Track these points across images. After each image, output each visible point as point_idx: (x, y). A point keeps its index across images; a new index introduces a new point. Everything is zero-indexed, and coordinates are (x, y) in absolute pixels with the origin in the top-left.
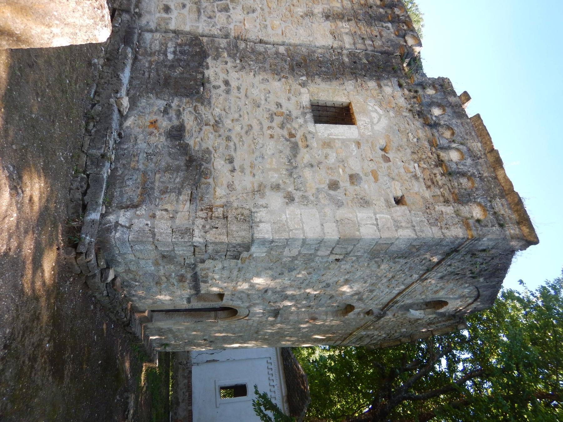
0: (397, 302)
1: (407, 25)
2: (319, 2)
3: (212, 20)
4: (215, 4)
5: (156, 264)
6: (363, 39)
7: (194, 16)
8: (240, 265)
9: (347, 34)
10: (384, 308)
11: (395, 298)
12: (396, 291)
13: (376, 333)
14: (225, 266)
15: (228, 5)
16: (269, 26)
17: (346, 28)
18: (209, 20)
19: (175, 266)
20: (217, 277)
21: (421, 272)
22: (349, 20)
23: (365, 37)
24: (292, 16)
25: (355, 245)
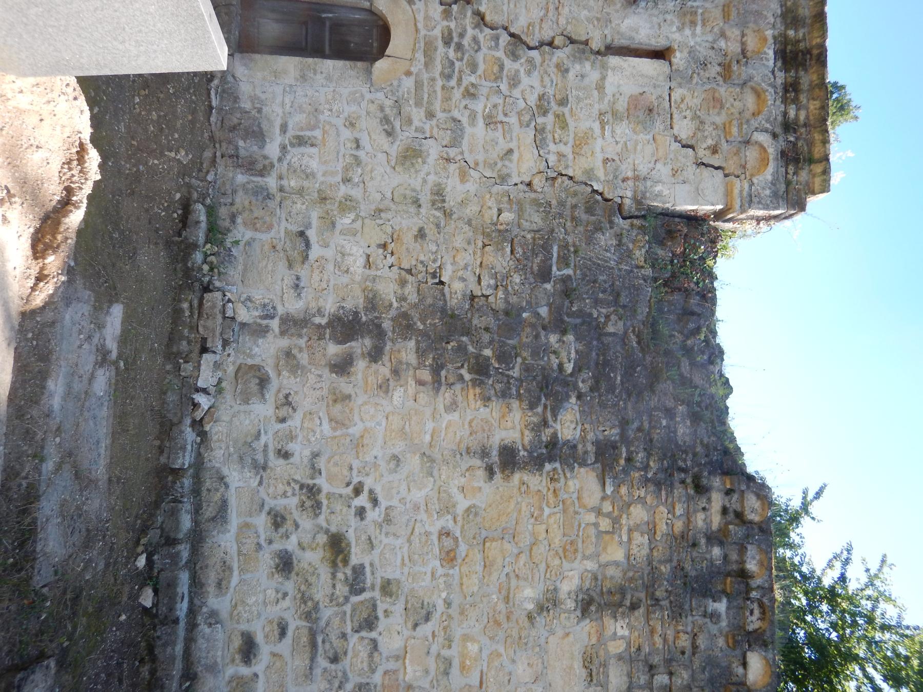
1: (761, 605)
2: (576, 551)
3: (339, 666)
4: (348, 608)
6: (651, 667)
7: (300, 662)
9: (620, 658)
15: (375, 606)
16: (456, 663)
17: (623, 637)
18: (333, 666)
22: (634, 607)
23: (656, 660)
24: (508, 618)
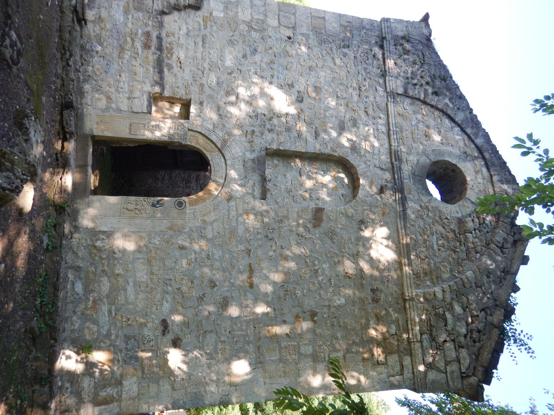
0: (399, 159)
5: (126, 12)
8: (203, 32)
10: (394, 179)
11: (390, 145)
12: (384, 129)
13: (438, 289)
14: (190, 28)
19: (143, 16)
20: (182, 56)
21: (381, 81)
25: (294, 14)
